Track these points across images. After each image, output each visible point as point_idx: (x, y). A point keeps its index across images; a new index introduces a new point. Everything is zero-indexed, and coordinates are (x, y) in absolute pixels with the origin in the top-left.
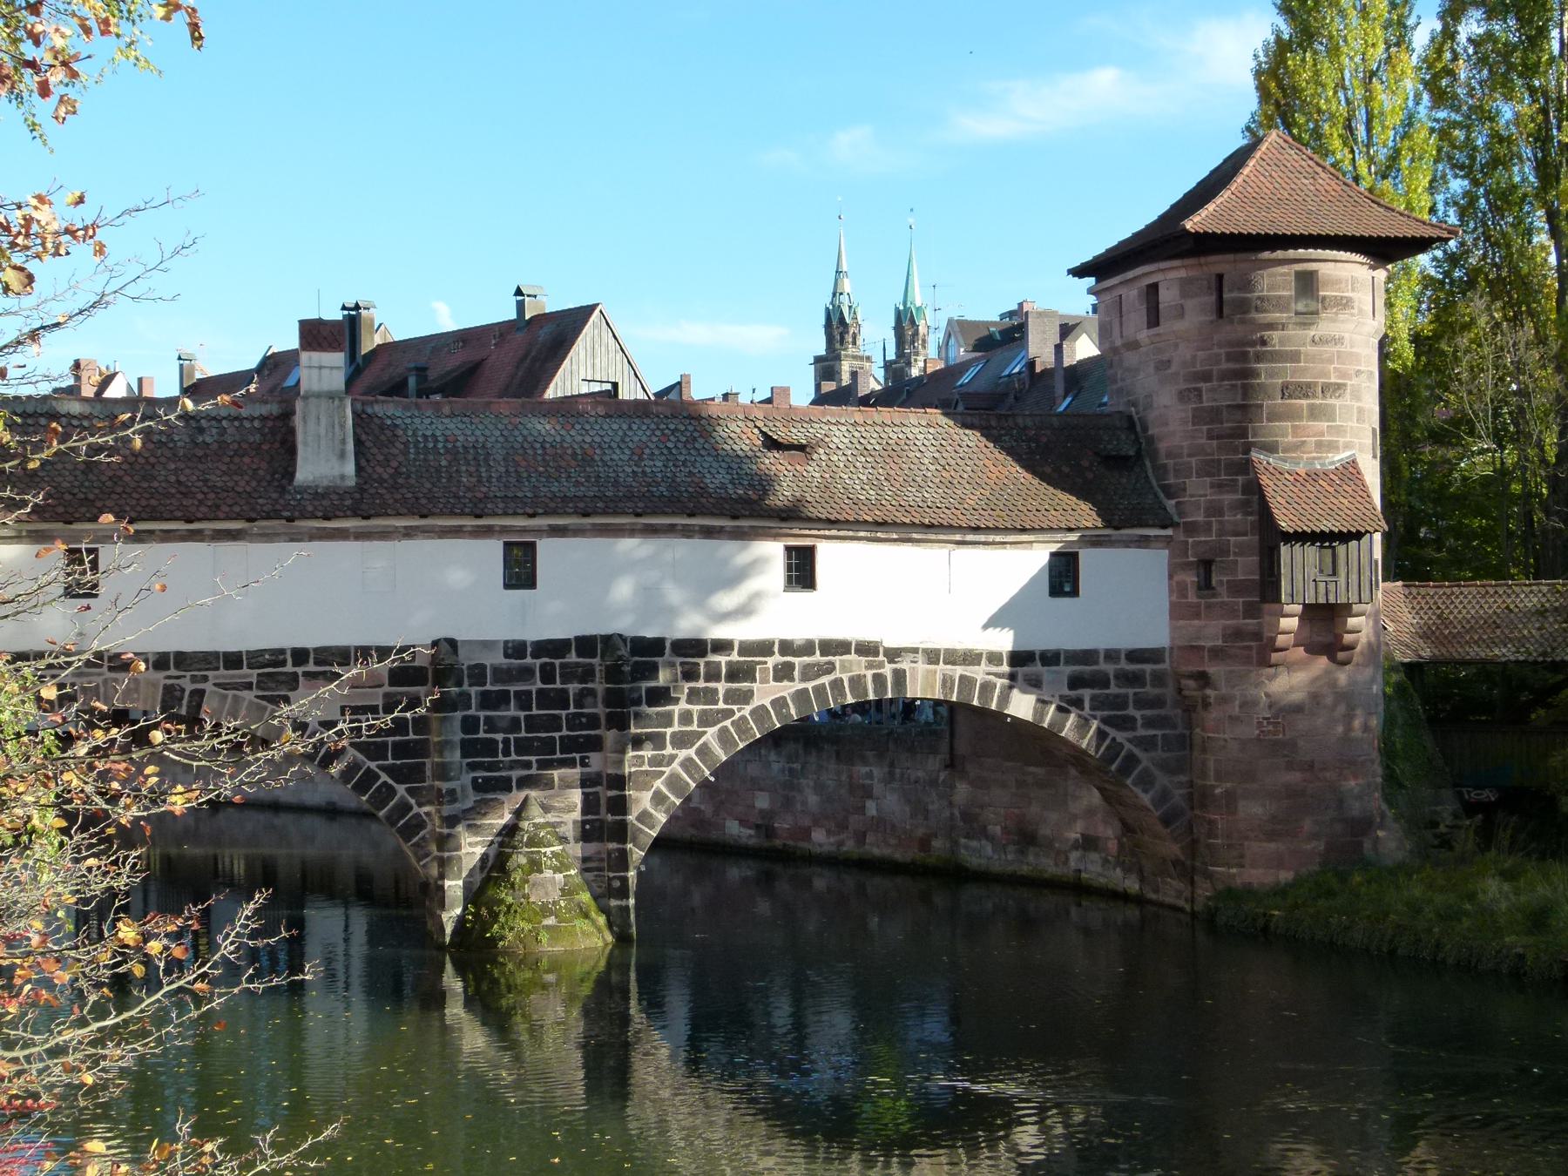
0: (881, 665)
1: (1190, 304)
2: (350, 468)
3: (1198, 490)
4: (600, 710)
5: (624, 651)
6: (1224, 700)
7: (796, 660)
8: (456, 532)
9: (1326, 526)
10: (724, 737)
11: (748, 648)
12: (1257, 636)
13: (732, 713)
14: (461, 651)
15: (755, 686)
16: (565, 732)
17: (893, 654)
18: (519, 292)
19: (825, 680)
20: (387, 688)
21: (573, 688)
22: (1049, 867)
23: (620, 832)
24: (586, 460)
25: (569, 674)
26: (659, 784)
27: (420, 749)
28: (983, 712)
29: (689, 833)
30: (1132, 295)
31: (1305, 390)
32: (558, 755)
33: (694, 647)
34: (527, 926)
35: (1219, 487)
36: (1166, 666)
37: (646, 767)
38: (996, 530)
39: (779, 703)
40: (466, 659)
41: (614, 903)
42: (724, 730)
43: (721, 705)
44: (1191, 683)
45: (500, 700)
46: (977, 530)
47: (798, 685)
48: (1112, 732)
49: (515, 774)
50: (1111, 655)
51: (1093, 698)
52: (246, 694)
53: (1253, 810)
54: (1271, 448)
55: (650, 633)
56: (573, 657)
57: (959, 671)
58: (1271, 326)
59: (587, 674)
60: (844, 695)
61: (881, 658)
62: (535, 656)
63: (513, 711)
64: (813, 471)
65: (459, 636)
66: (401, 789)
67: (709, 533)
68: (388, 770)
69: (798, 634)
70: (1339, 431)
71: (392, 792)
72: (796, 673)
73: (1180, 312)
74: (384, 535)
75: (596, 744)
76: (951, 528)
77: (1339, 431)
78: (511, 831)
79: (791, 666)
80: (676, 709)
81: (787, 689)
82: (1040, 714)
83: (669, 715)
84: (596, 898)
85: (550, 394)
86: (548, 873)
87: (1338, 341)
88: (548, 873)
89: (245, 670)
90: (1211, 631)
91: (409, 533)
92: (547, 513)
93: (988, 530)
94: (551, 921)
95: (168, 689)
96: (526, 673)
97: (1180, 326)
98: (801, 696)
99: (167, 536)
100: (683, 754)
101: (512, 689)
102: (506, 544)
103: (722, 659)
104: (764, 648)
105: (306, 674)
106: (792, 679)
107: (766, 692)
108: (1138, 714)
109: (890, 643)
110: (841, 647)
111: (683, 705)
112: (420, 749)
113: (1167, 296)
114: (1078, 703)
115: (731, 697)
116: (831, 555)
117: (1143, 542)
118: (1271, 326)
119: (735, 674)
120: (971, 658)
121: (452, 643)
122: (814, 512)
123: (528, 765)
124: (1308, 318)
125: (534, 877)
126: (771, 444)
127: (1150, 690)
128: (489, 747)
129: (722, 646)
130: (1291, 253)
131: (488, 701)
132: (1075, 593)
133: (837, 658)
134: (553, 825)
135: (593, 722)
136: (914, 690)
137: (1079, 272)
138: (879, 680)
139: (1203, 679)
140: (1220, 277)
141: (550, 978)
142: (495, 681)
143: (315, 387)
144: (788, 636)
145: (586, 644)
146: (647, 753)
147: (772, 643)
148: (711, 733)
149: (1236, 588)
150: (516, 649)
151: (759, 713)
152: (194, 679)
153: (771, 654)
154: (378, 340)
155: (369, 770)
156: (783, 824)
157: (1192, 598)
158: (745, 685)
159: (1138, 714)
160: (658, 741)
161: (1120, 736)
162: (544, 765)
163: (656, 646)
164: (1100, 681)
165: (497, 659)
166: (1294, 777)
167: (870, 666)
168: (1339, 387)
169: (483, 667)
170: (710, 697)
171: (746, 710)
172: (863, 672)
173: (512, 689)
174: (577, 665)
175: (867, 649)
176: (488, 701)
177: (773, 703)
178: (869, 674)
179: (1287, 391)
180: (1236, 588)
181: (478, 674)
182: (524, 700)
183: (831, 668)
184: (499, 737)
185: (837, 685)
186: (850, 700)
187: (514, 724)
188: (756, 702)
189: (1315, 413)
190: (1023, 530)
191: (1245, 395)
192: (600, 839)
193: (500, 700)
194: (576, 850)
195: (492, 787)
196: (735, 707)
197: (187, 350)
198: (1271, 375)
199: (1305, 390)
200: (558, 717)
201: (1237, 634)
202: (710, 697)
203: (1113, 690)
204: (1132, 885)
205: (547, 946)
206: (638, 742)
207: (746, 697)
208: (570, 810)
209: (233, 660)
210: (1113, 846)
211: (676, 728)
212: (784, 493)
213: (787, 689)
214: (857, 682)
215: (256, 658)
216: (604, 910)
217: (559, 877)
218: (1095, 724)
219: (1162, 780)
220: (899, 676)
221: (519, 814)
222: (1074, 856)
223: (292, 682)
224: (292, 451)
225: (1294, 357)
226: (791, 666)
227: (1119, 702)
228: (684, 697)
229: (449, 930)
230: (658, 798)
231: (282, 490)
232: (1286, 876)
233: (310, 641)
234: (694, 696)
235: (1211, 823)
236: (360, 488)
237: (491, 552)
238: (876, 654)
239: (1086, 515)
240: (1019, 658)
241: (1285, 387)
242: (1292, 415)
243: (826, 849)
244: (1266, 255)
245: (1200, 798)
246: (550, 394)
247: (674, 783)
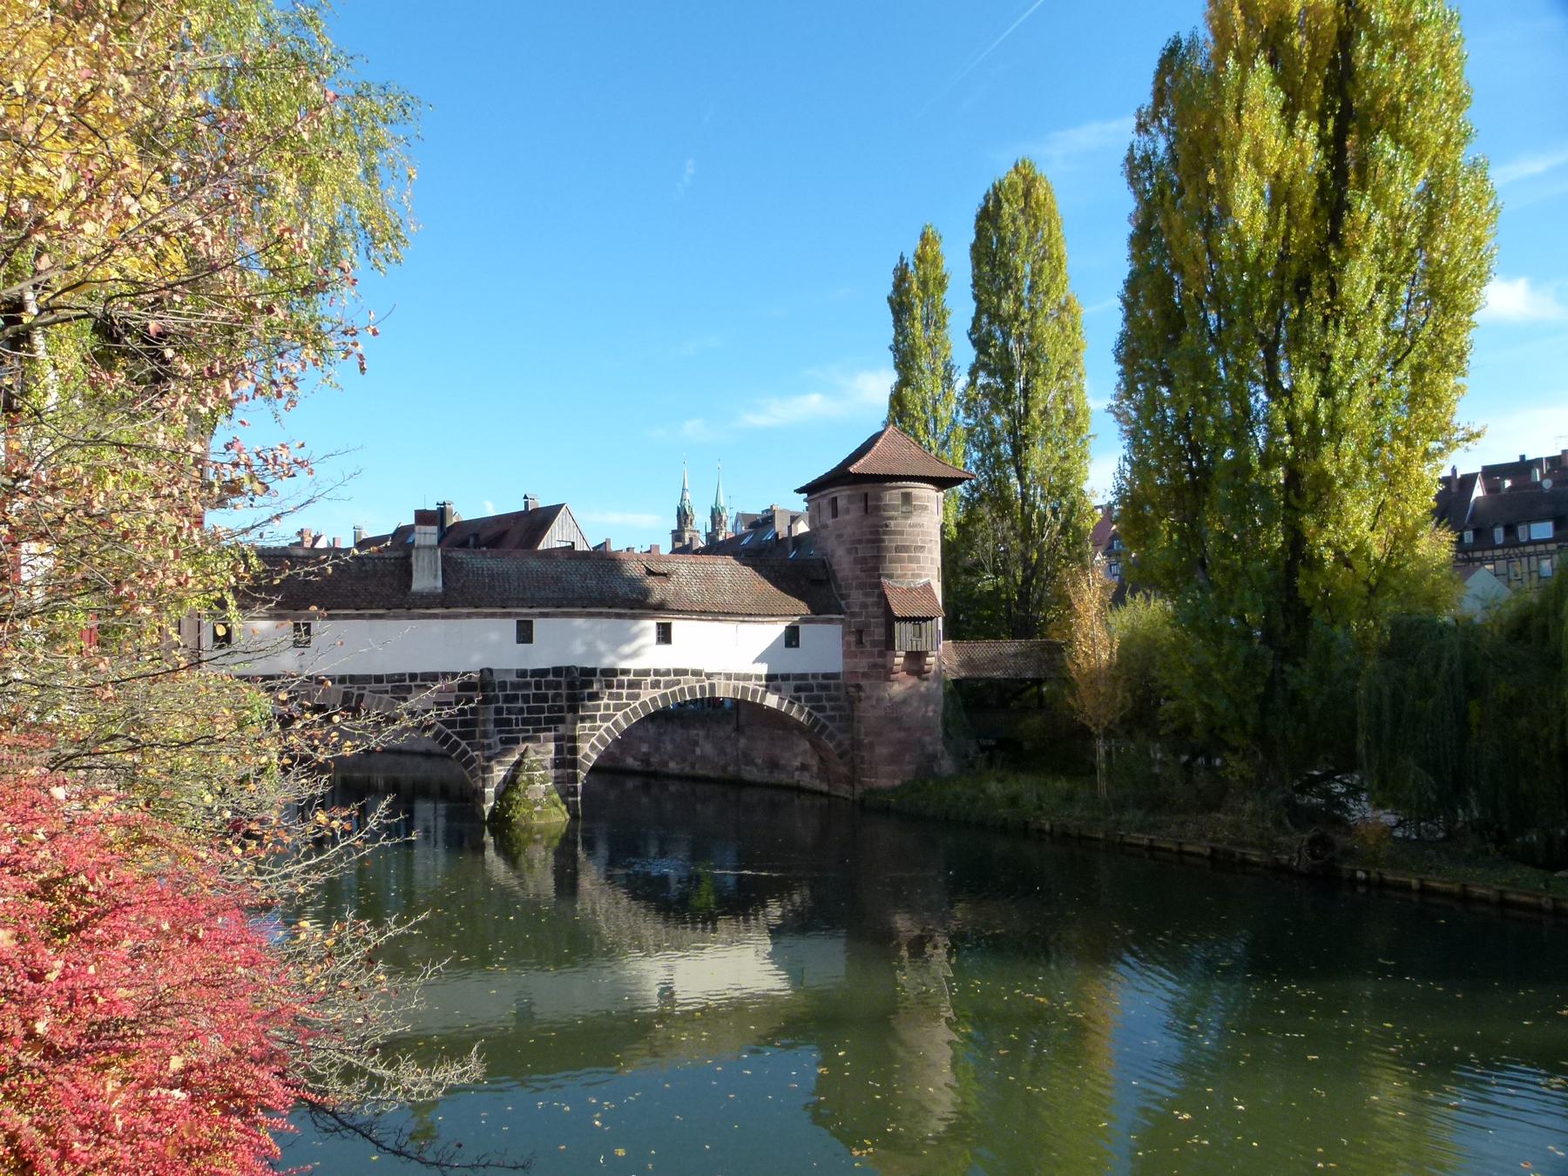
1: (853, 507)
2: (439, 583)
3: (856, 597)
4: (564, 703)
5: (576, 675)
6: (869, 697)
7: (662, 679)
8: (493, 615)
9: (917, 614)
10: (626, 716)
11: (638, 673)
12: (884, 666)
17: (709, 676)
18: (525, 497)
19: (676, 688)
20: (457, 693)
21: (551, 692)
22: (783, 778)
23: (574, 764)
24: (559, 580)
25: (549, 685)
26: (593, 740)
27: (473, 723)
28: (753, 704)
29: (608, 764)
30: (825, 502)
31: (905, 549)
33: (611, 672)
34: (526, 811)
35: (866, 595)
36: (840, 681)
38: (759, 615)
39: (653, 700)
40: (497, 679)
41: (570, 799)
43: (625, 701)
44: (852, 689)
45: (514, 698)
46: (750, 615)
48: (815, 713)
49: (521, 735)
50: (815, 676)
51: (806, 697)
52: (385, 696)
53: (882, 751)
54: (890, 576)
55: (589, 666)
56: (551, 678)
57: (741, 684)
58: (891, 518)
59: (558, 685)
63: (520, 704)
64: (670, 586)
66: (464, 743)
67: (619, 616)
68: (458, 734)
69: (662, 666)
70: (923, 568)
71: (459, 744)
73: (847, 511)
74: (456, 616)
75: (562, 720)
76: (737, 614)
77: (923, 568)
78: (519, 764)
79: (659, 681)
80: (602, 703)
81: (657, 693)
82: (780, 705)
83: (599, 705)
84: (561, 796)
85: (540, 547)
86: (537, 785)
87: (921, 526)
88: (537, 785)
89: (385, 684)
90: (862, 664)
91: (469, 616)
92: (538, 606)
93: (755, 615)
94: (538, 808)
95: (346, 694)
96: (527, 685)
97: (847, 517)
98: (664, 696)
99: (346, 617)
100: (605, 725)
102: (519, 622)
103: (625, 678)
104: (646, 673)
107: (646, 695)
108: (827, 704)
109: (708, 670)
110: (684, 672)
111: (606, 701)
112: (473, 723)
113: (841, 503)
114: (799, 699)
115: (629, 697)
116: (679, 627)
117: (830, 621)
118: (891, 518)
119: (631, 685)
120: (747, 677)
121: (490, 671)
122: (671, 607)
123: (528, 731)
124: (908, 514)
125: (530, 786)
126: (650, 573)
127: (833, 693)
128: (509, 722)
129: (625, 672)
130: (899, 484)
131: (508, 699)
132: (797, 645)
134: (541, 761)
135: (561, 709)
136: (719, 694)
137: (800, 491)
138: (702, 688)
139: (859, 687)
140: (866, 495)
141: (538, 836)
143: (422, 543)
145: (557, 671)
146: (588, 725)
149: (874, 644)
150: (522, 673)
151: (644, 705)
152: (359, 689)
154: (455, 520)
155: (447, 734)
156: (654, 759)
157: (853, 648)
159: (827, 704)
160: (593, 718)
161: (819, 715)
162: (536, 731)
163: (592, 672)
164: (809, 688)
165: (514, 679)
166: (902, 735)
167: (698, 681)
168: (922, 547)
169: (505, 683)
170: (619, 696)
171: (637, 703)
175: (696, 673)
176: (508, 699)
179: (899, 549)
180: (874, 644)
181: (503, 686)
182: (526, 699)
183: (678, 682)
184: (514, 717)
185: (682, 691)
186: (688, 698)
187: (521, 711)
188: (642, 700)
189: (911, 560)
190: (773, 615)
191: (879, 551)
192: (564, 767)
193: (514, 698)
194: (552, 773)
195: (509, 742)
197: (358, 524)
198: (890, 541)
199: (905, 549)
201: (875, 666)
202: (619, 696)
203: (816, 692)
204: (824, 787)
205: (537, 821)
206: (583, 719)
207: (637, 697)
208: (550, 752)
210: (815, 769)
212: (656, 597)
213: (657, 693)
214: (692, 690)
215: (391, 678)
216: (565, 802)
217: (543, 786)
218: (807, 709)
219: (840, 736)
220: (712, 686)
221: (523, 755)
222: (797, 773)
223: (409, 690)
224: (410, 575)
225: (901, 533)
226: (659, 681)
227: (819, 699)
229: (487, 814)
230: (593, 747)
231: (405, 594)
232: (897, 782)
233: (418, 670)
234: (611, 696)
235: (863, 757)
236: (445, 593)
237: (511, 625)
239: (803, 608)
240: (770, 678)
241: (897, 547)
242: (901, 561)
243: (677, 771)
244: (888, 484)
245: (856, 745)
246: (540, 547)
247: (601, 739)
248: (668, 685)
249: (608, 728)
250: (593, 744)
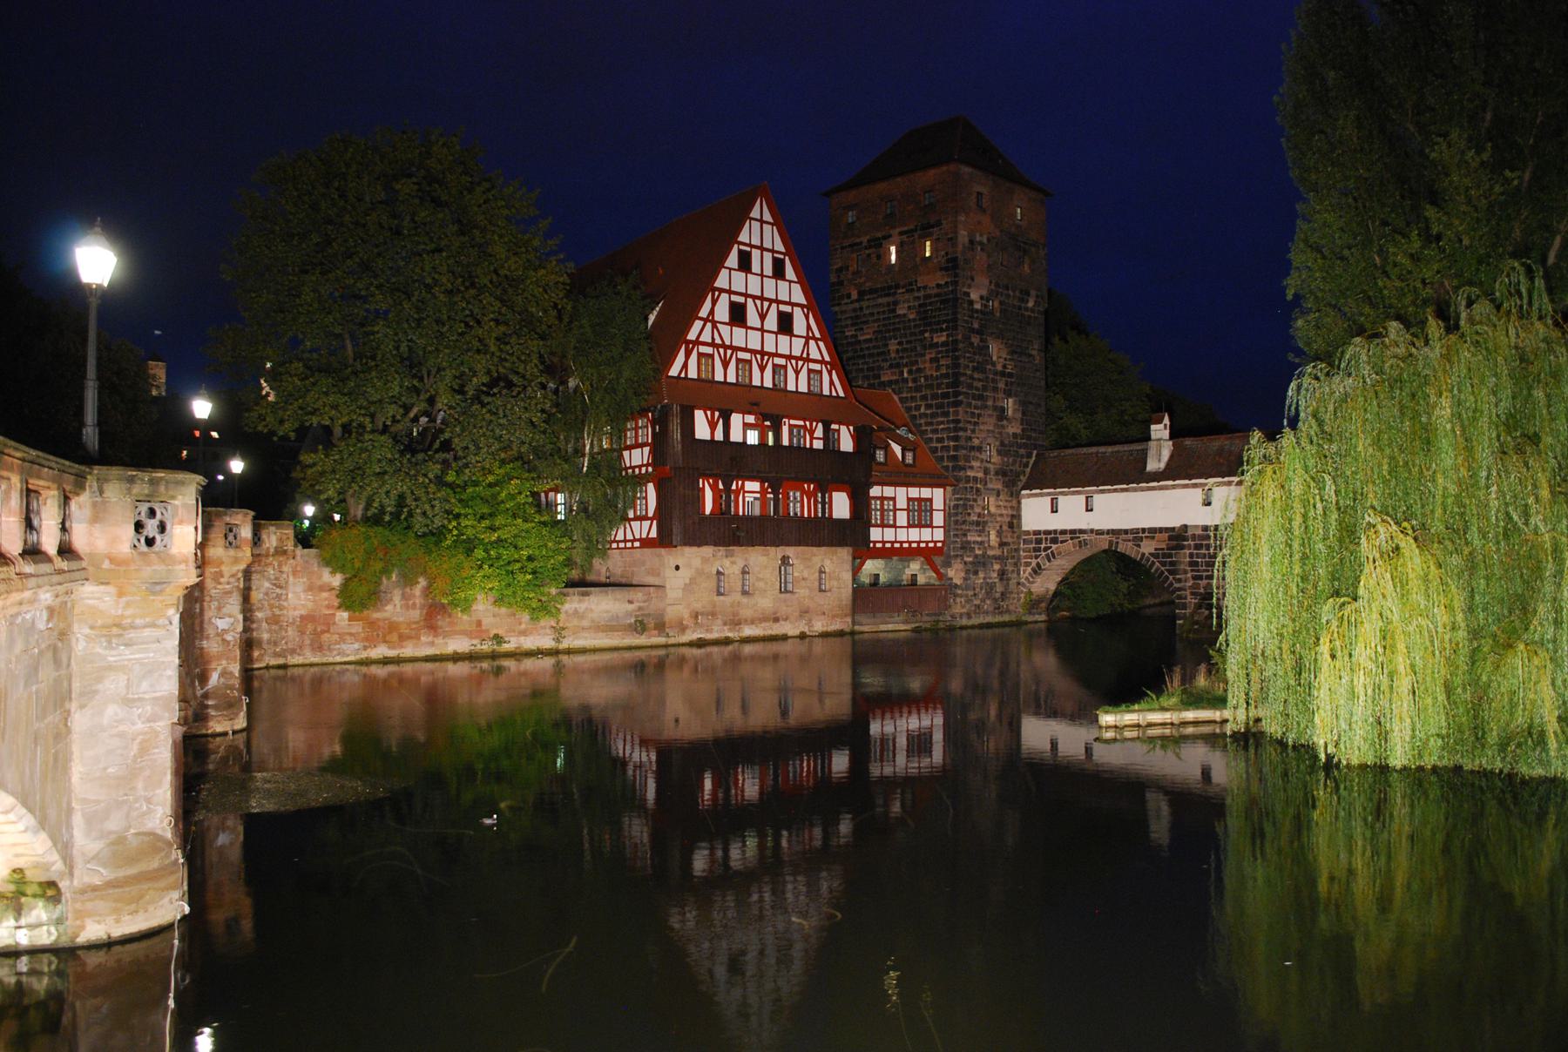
2: (1162, 465)
14: (1189, 529)
49: (1205, 574)
52: (1130, 544)
65: (1189, 523)
66: (1171, 577)
68: (1167, 570)
71: (1168, 578)
101: (1204, 542)
105: (1146, 537)
128: (1196, 564)
131: (1198, 547)
173: (1204, 542)
209: (1126, 532)
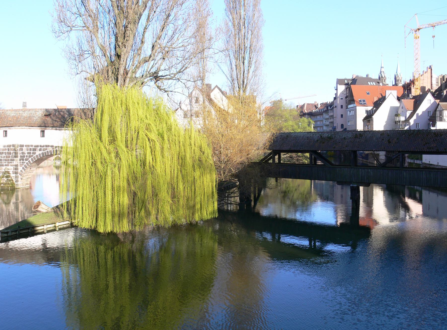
0: (54, 149)
7: (42, 148)
10: (32, 159)
13: (33, 156)
15: (36, 152)
16: (11, 158)
19: (46, 151)
26: (23, 166)
32: (10, 161)
37: (21, 164)
39: (40, 154)
42: (32, 158)
43: (32, 155)
47: (42, 152)
55: (22, 144)
56: (12, 147)
60: (49, 153)
61: (54, 148)
62: (7, 147)
63: (4, 155)
72: (42, 150)
79: (41, 149)
83: (25, 156)
88: (4, 178)
100: (26, 162)
101: (4, 152)
104: (38, 146)
106: (41, 151)
107: (38, 153)
109: (55, 145)
110: (49, 146)
133: (48, 148)
142: (2, 151)
144: (41, 145)
147: (38, 146)
148: (30, 159)
151: (37, 156)
153: (38, 147)
158: (35, 152)
162: (8, 163)
172: (51, 150)
173: (4, 152)
174: (12, 148)
175: (52, 146)
177: (39, 154)
178: (52, 150)
182: (5, 153)
183: (47, 149)
184: (2, 159)
185: (48, 152)
186: (49, 154)
188: (36, 154)
196: (33, 155)
200: (10, 156)
207: (34, 153)
208: (11, 169)
211: (26, 158)
213: (41, 152)
228: (27, 153)
238: (53, 147)
248: (44, 150)
249: (27, 163)
250: (23, 167)
